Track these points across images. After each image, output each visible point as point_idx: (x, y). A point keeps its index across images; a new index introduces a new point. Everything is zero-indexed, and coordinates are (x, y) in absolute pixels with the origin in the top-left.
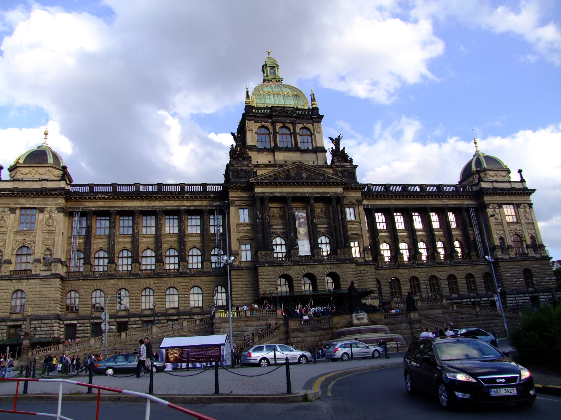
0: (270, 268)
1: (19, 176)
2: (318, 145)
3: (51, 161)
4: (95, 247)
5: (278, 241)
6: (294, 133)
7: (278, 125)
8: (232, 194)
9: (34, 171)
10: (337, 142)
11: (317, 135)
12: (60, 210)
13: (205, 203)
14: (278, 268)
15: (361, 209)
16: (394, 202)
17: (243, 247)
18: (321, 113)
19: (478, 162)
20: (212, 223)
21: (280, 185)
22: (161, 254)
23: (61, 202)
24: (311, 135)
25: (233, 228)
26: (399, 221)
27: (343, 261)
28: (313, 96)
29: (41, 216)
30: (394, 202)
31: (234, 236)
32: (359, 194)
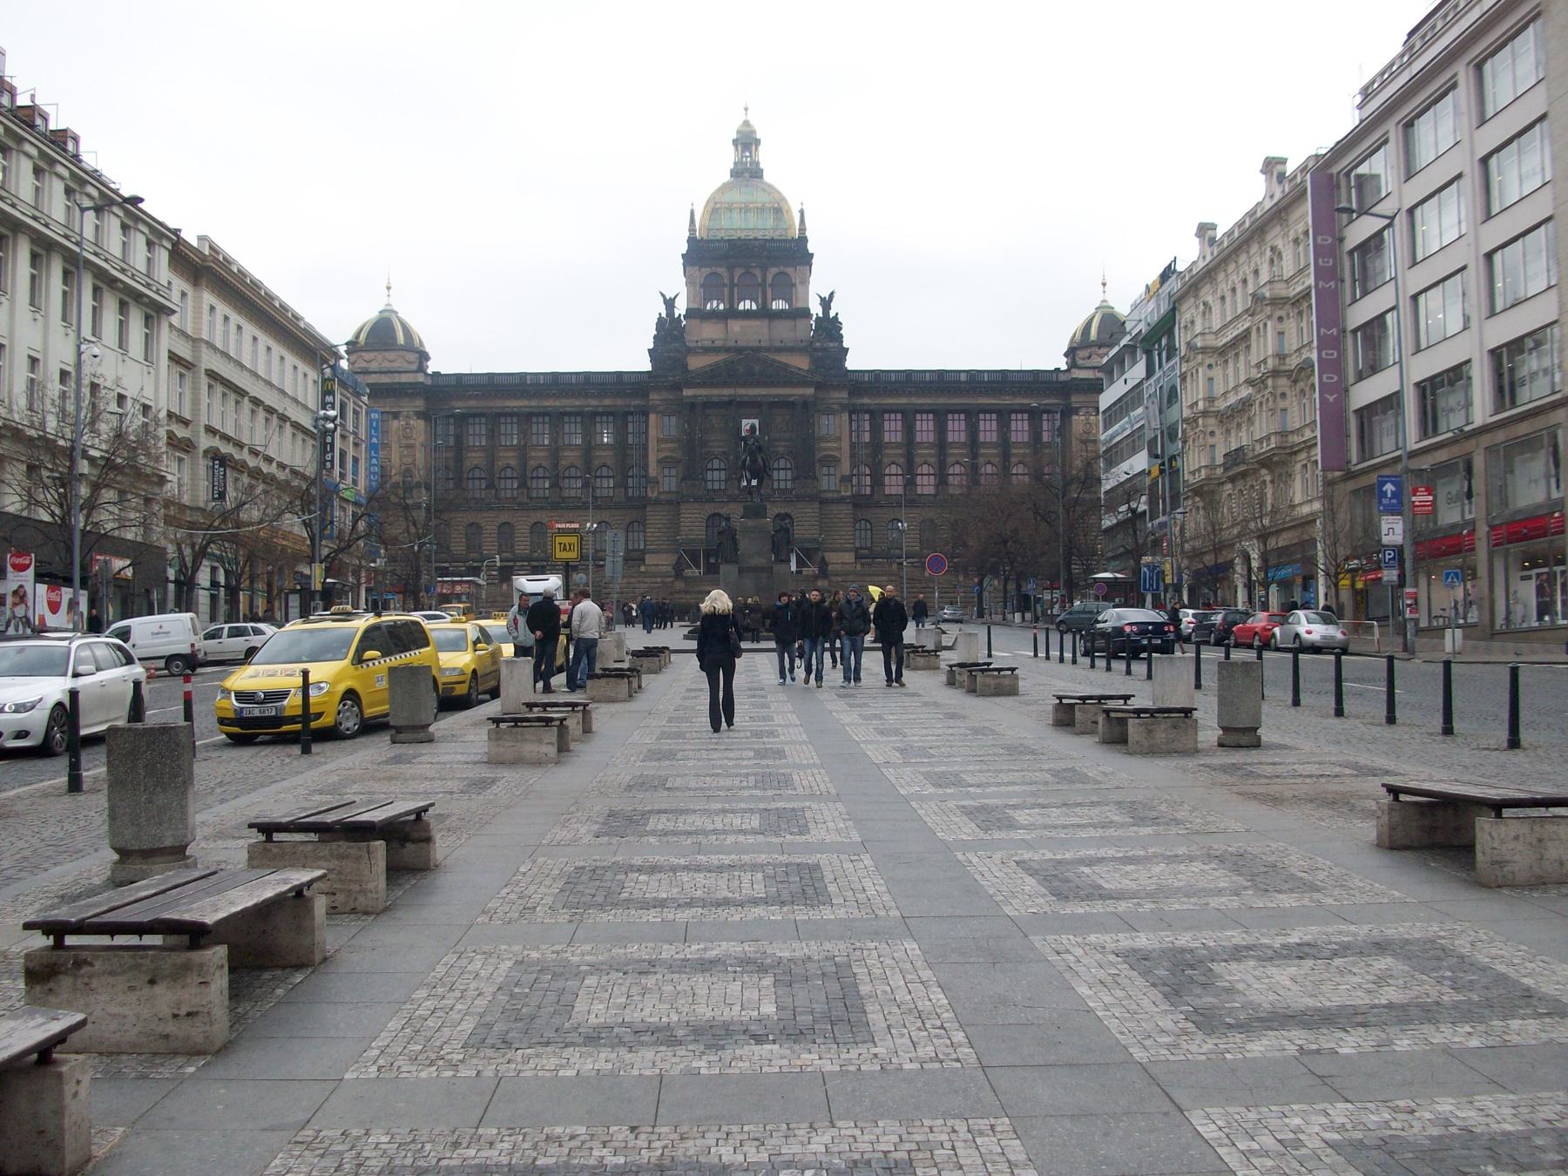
0: (696, 505)
1: (362, 364)
2: (800, 305)
3: (401, 339)
4: (468, 464)
5: (716, 464)
6: (763, 285)
7: (738, 272)
8: (654, 396)
9: (379, 356)
10: (826, 303)
11: (799, 287)
12: (419, 415)
13: (619, 402)
14: (707, 506)
15: (845, 417)
16: (914, 400)
17: (666, 471)
18: (811, 248)
19: (1087, 328)
20: (630, 429)
21: (725, 385)
22: (557, 476)
23: (420, 404)
24: (794, 285)
25: (652, 445)
26: (925, 429)
27: (800, 498)
28: (802, 212)
29: (395, 423)
30: (914, 400)
31: (652, 458)
32: (845, 395)
